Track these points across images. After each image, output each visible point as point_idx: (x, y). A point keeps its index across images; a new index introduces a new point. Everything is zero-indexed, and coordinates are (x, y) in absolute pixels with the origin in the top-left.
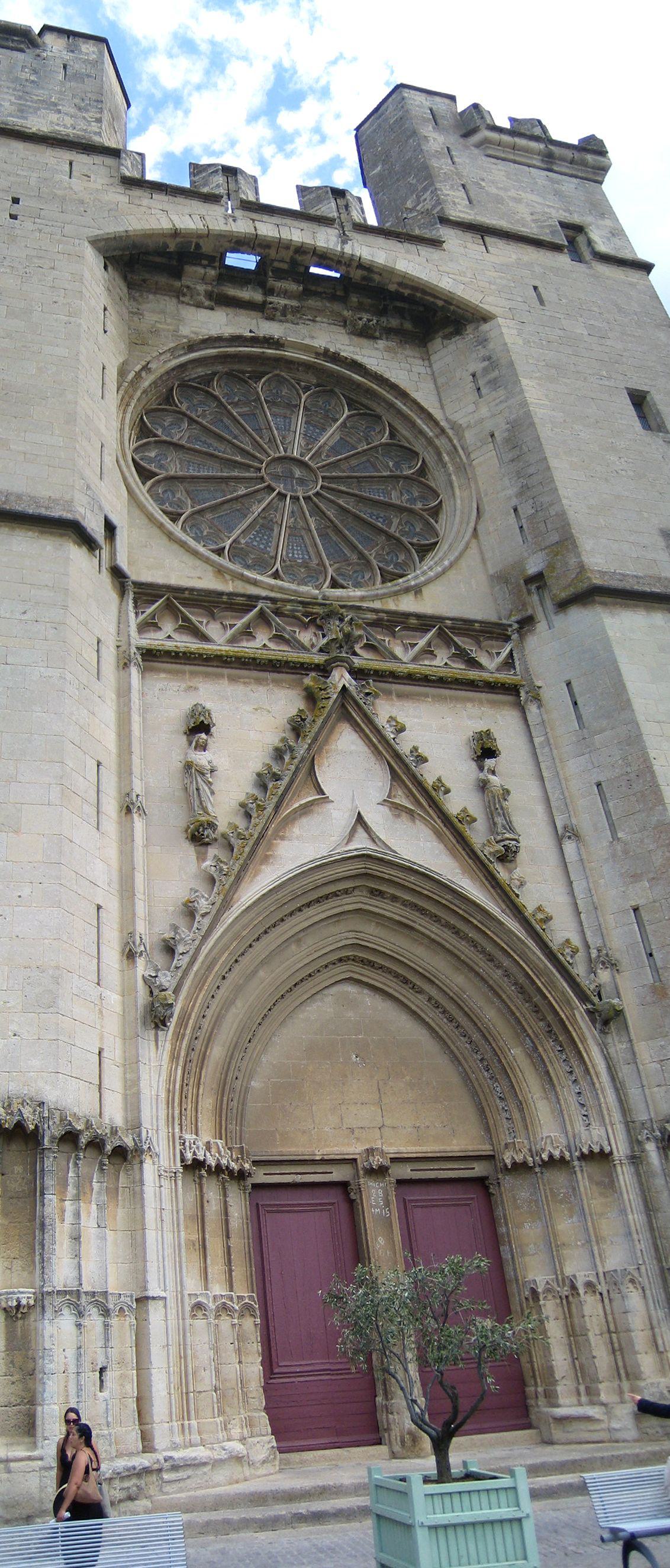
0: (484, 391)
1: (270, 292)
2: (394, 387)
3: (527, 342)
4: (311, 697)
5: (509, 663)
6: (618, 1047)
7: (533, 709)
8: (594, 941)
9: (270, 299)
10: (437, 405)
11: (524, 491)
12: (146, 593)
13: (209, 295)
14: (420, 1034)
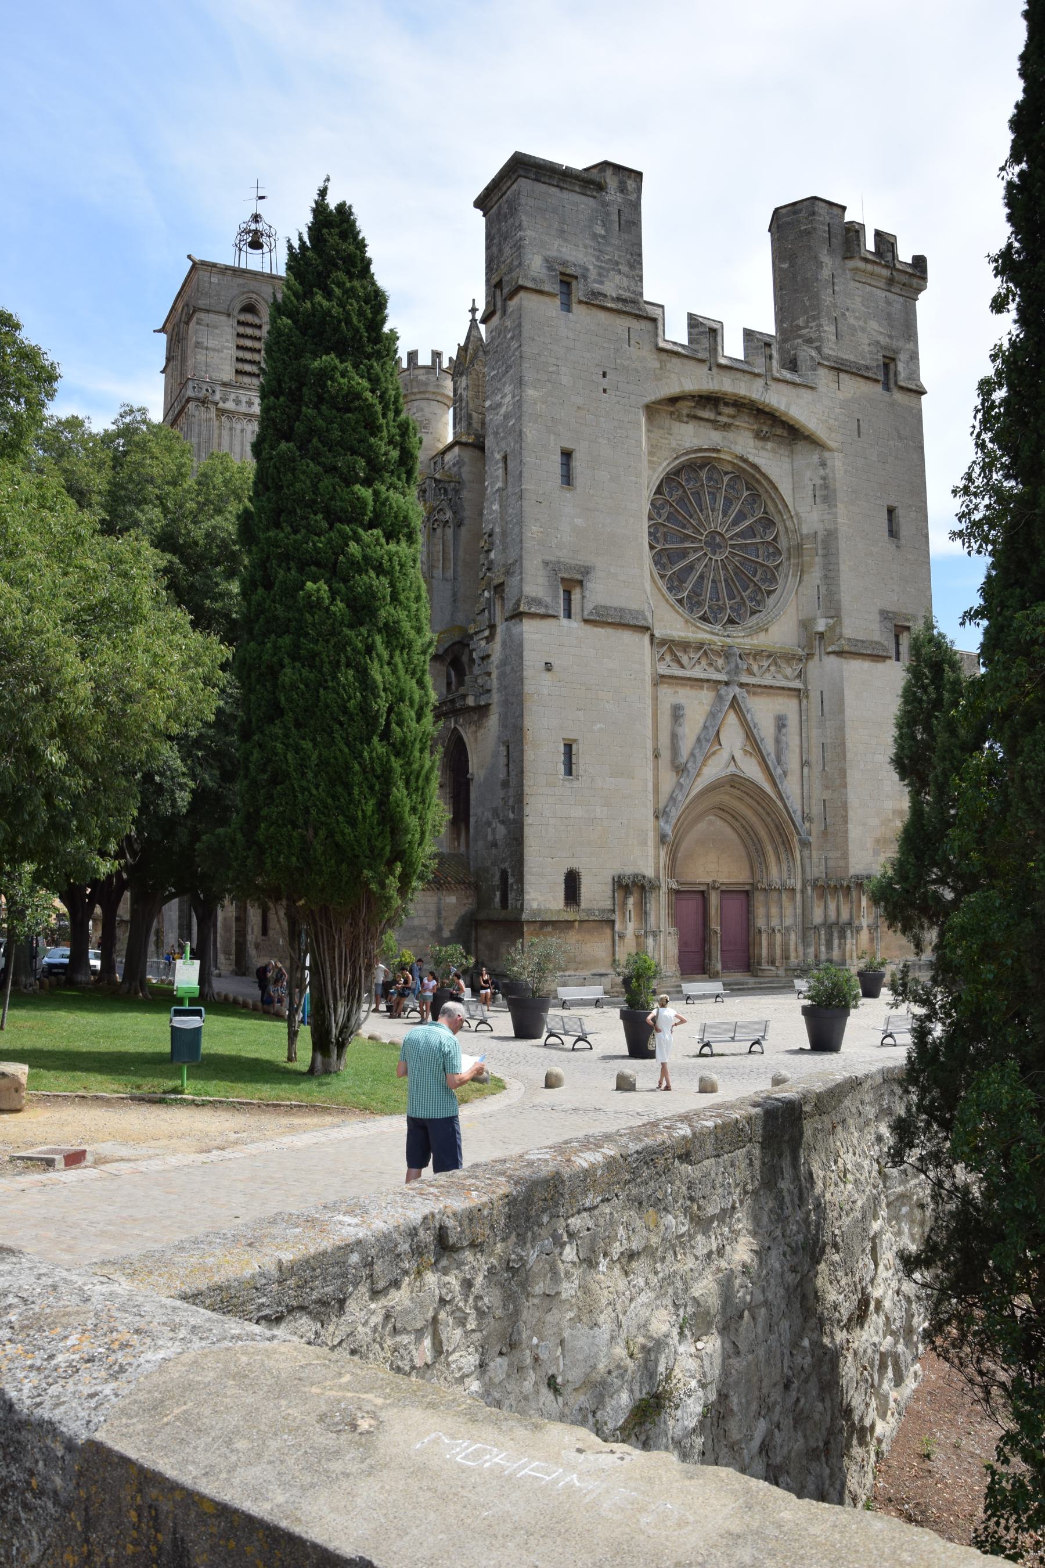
0: (818, 500)
1: (720, 414)
2: (771, 482)
3: (846, 471)
4: (720, 698)
5: (799, 676)
6: (806, 853)
7: (804, 702)
8: (806, 811)
9: (719, 418)
10: (790, 492)
11: (826, 577)
12: (663, 642)
13: (688, 416)
14: (737, 840)
